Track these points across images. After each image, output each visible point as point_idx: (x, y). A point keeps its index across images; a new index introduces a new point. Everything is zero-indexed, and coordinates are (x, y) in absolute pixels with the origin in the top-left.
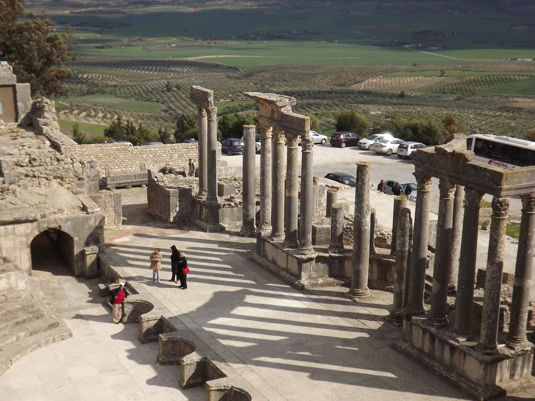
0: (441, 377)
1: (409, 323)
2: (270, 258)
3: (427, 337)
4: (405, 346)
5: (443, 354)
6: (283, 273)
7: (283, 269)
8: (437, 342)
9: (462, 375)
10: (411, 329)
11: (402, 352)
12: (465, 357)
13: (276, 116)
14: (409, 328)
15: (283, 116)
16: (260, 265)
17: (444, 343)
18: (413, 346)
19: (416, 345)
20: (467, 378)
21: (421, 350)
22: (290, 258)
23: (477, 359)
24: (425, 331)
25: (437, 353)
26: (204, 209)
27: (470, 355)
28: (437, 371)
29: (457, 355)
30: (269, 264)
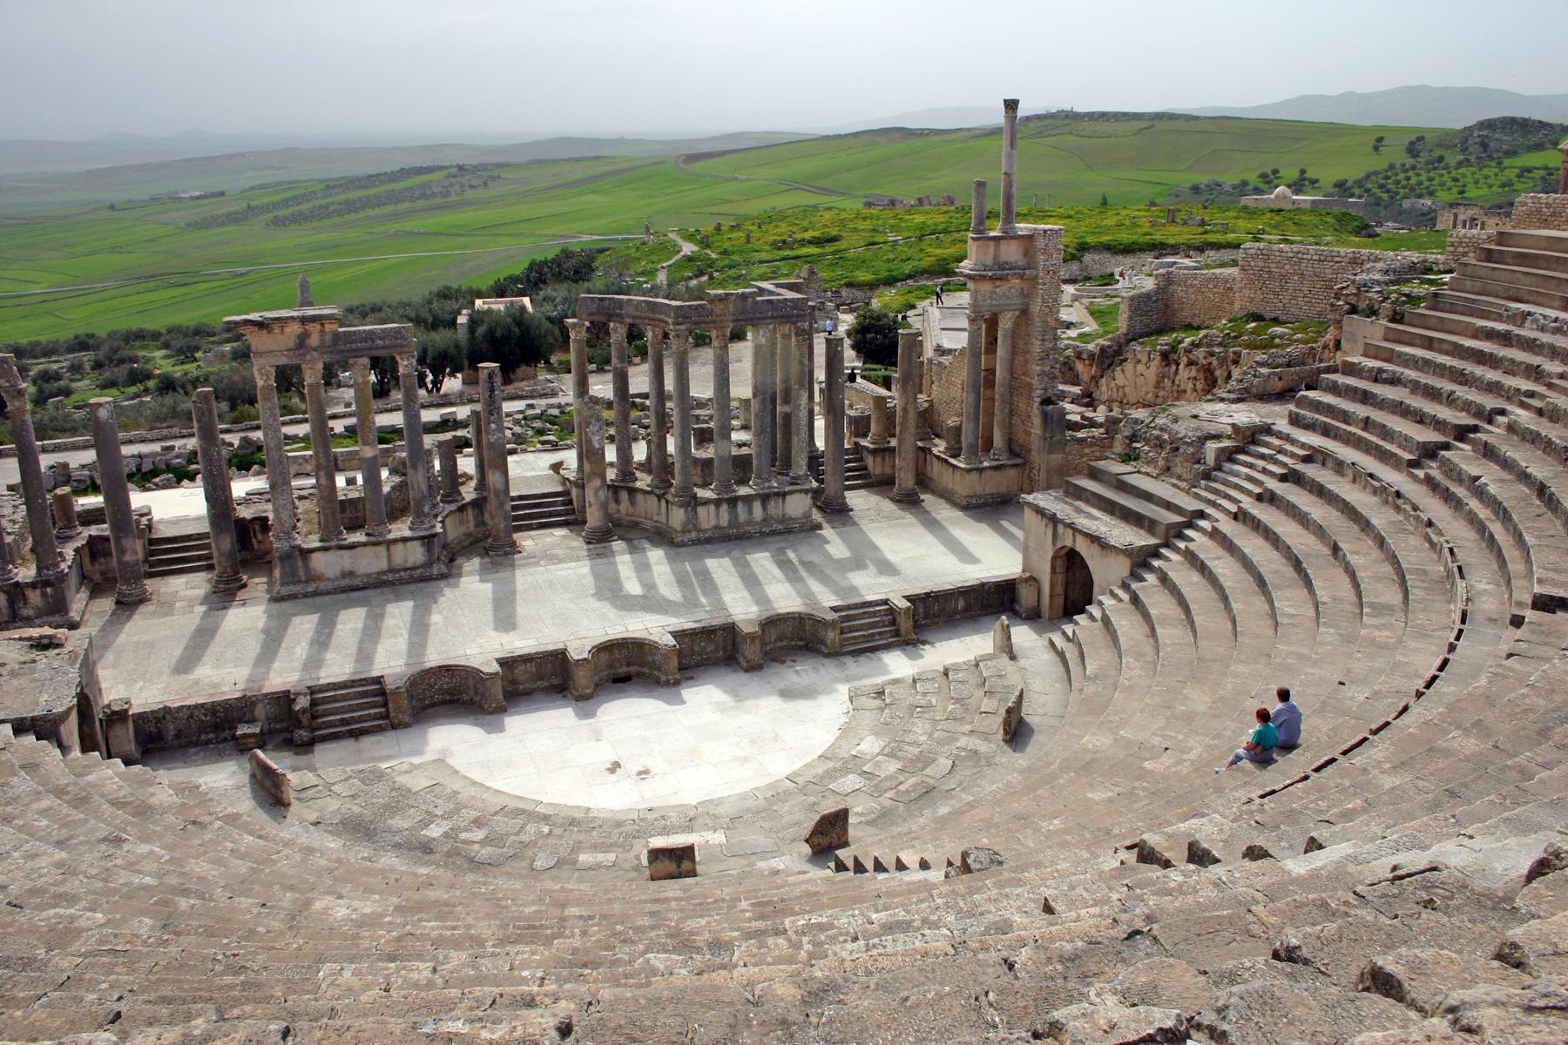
0: (762, 534)
2: (330, 573)
3: (725, 507)
4: (694, 535)
6: (390, 577)
7: (384, 573)
8: (740, 506)
9: (784, 519)
11: (695, 543)
13: (314, 340)
15: (337, 337)
16: (316, 594)
17: (748, 499)
18: (698, 531)
21: (717, 527)
23: (800, 491)
26: (34, 597)
27: (791, 493)
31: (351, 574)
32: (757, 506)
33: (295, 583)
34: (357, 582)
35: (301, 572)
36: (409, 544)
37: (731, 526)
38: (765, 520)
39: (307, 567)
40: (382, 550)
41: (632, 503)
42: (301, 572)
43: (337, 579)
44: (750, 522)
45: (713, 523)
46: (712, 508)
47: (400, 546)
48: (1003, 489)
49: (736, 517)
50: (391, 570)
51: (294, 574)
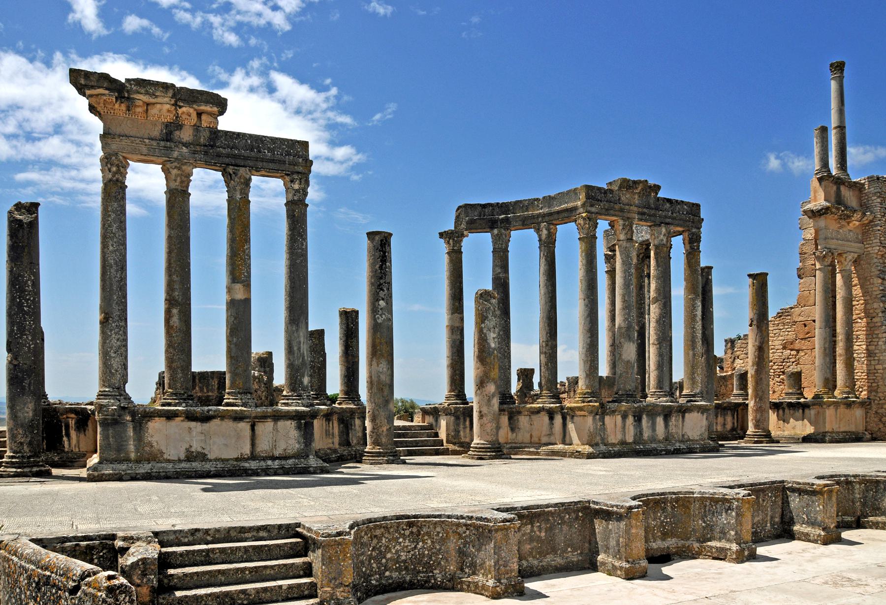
1: (598, 417)
3: (630, 420)
4: (603, 448)
5: (654, 430)
6: (253, 465)
10: (604, 424)
12: (683, 417)
14: (599, 424)
19: (614, 441)
20: (689, 440)
21: (623, 443)
22: (265, 428)
24: (624, 417)
25: (646, 434)
28: (661, 451)
29: (673, 420)
30: (183, 465)
31: (202, 457)
32: (660, 421)
33: (120, 461)
34: (208, 466)
35: (131, 447)
36: (281, 423)
37: (635, 442)
38: (667, 439)
39: (139, 439)
40: (244, 427)
41: (513, 428)
42: (131, 447)
43: (180, 461)
44: (653, 439)
45: (619, 437)
46: (619, 418)
47: (269, 425)
48: (852, 428)
49: (641, 433)
50: (253, 457)
51: (120, 447)
